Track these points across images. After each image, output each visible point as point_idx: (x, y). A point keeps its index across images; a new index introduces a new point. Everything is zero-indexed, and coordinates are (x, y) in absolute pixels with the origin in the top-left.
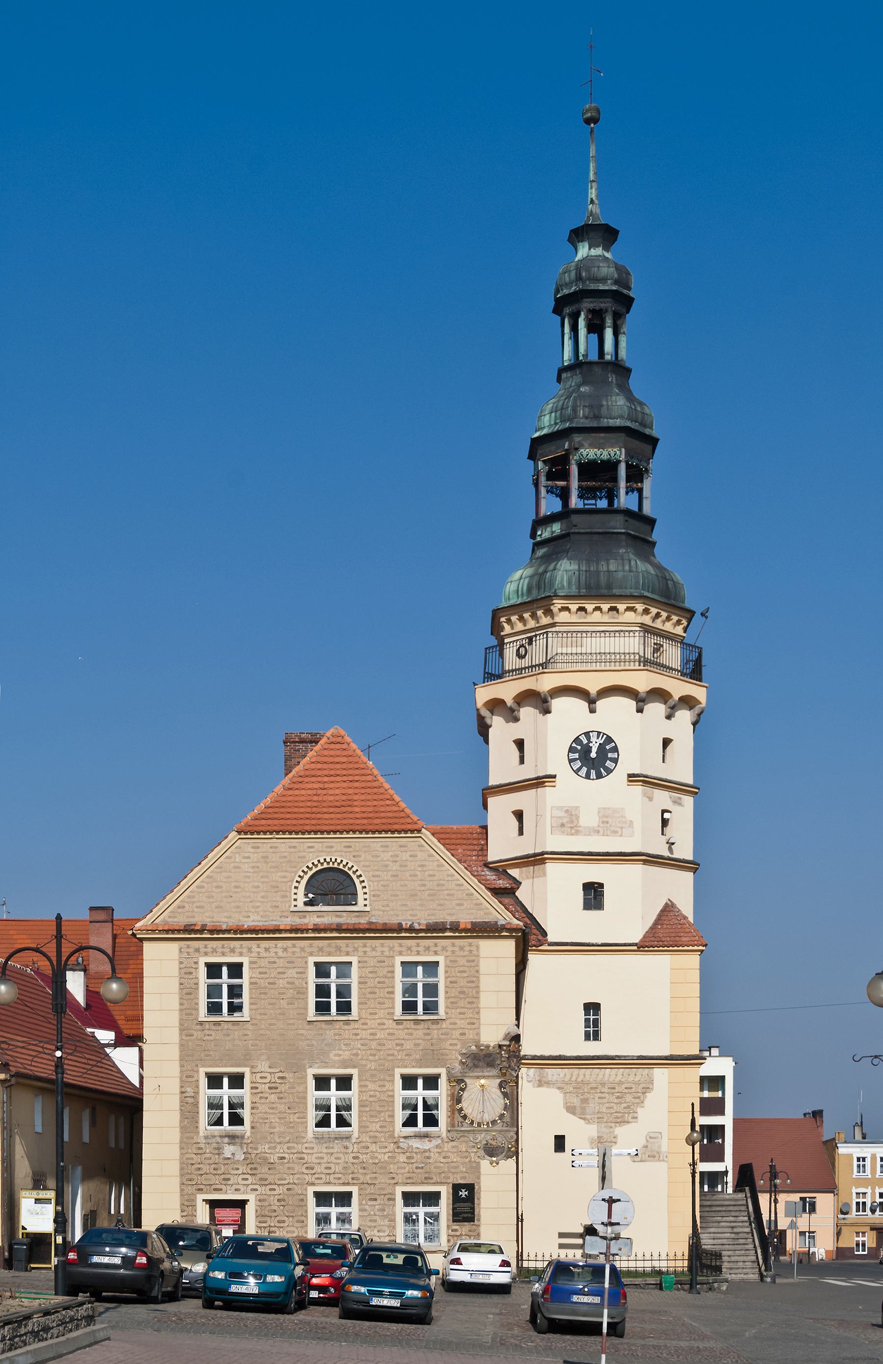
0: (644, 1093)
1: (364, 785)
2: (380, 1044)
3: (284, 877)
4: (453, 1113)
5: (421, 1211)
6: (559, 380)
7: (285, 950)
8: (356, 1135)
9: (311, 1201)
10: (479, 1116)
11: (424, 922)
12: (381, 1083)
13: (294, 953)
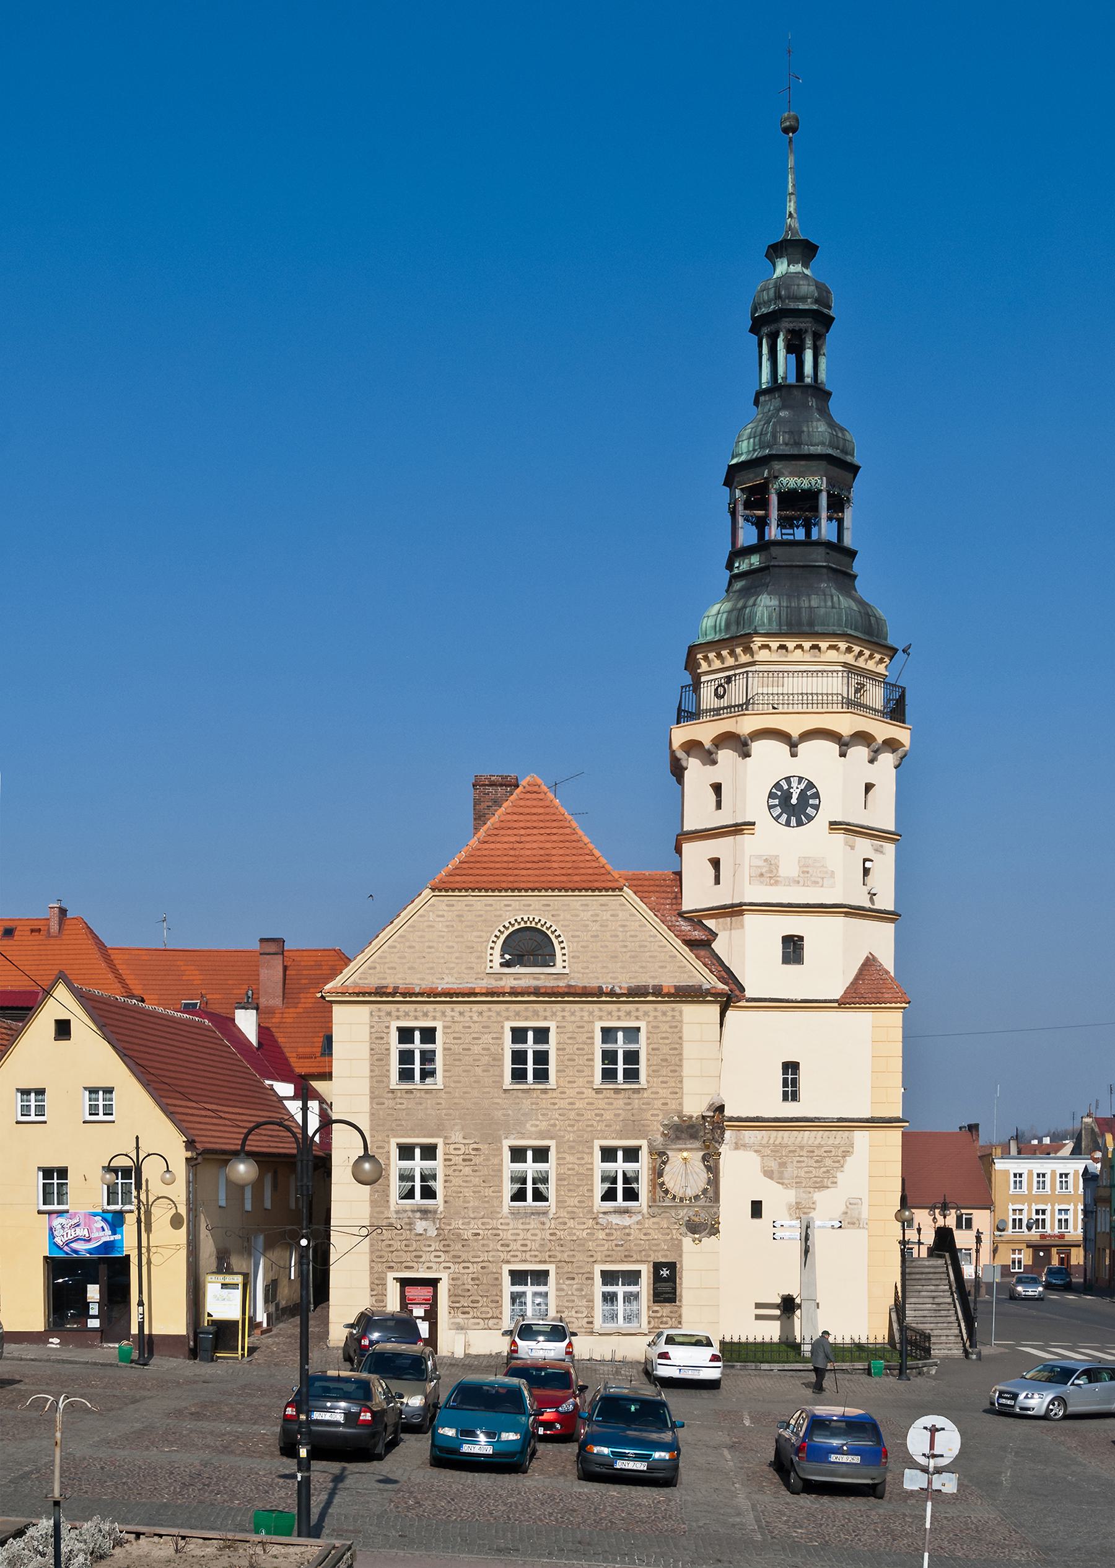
1: (562, 838)
2: (578, 1115)
3: (480, 937)
4: (654, 1188)
5: (620, 1290)
6: (756, 403)
7: (481, 1013)
8: (553, 1210)
9: (507, 1279)
10: (682, 1191)
11: (625, 985)
12: (579, 1156)
13: (489, 1017)
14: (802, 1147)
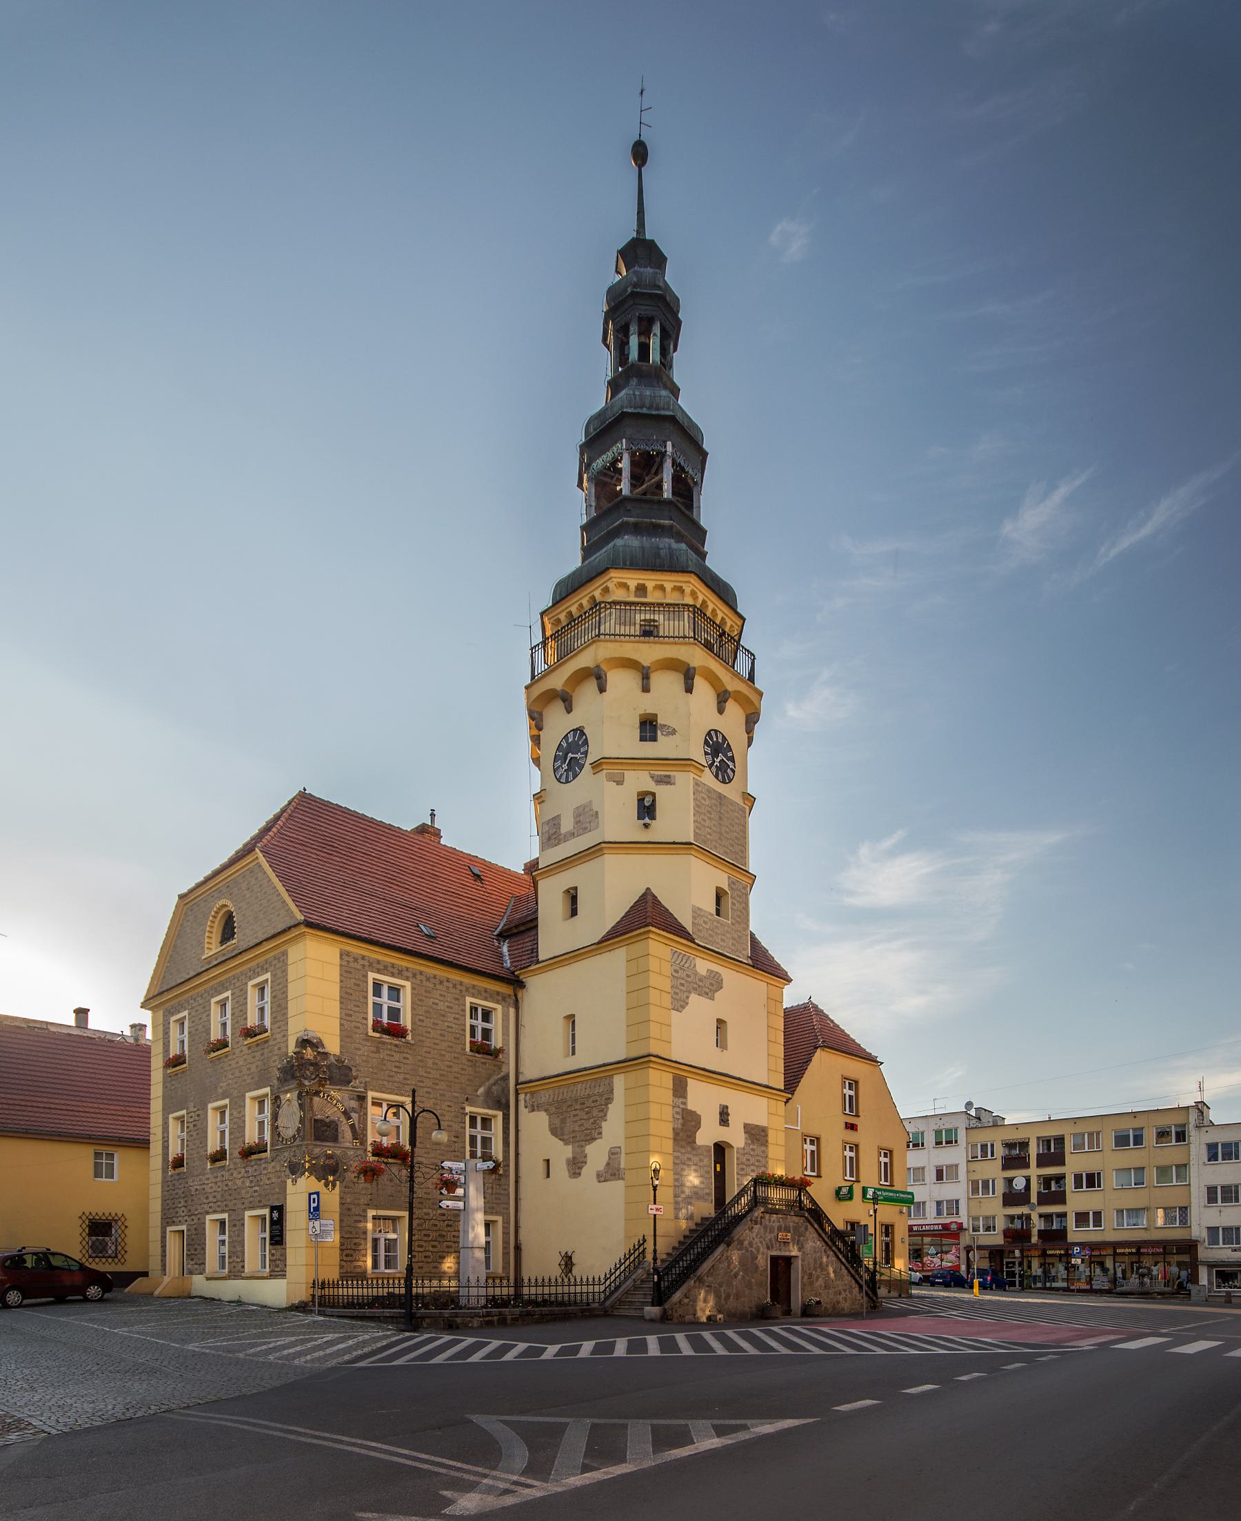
0: (606, 1105)
14: (576, 1101)
